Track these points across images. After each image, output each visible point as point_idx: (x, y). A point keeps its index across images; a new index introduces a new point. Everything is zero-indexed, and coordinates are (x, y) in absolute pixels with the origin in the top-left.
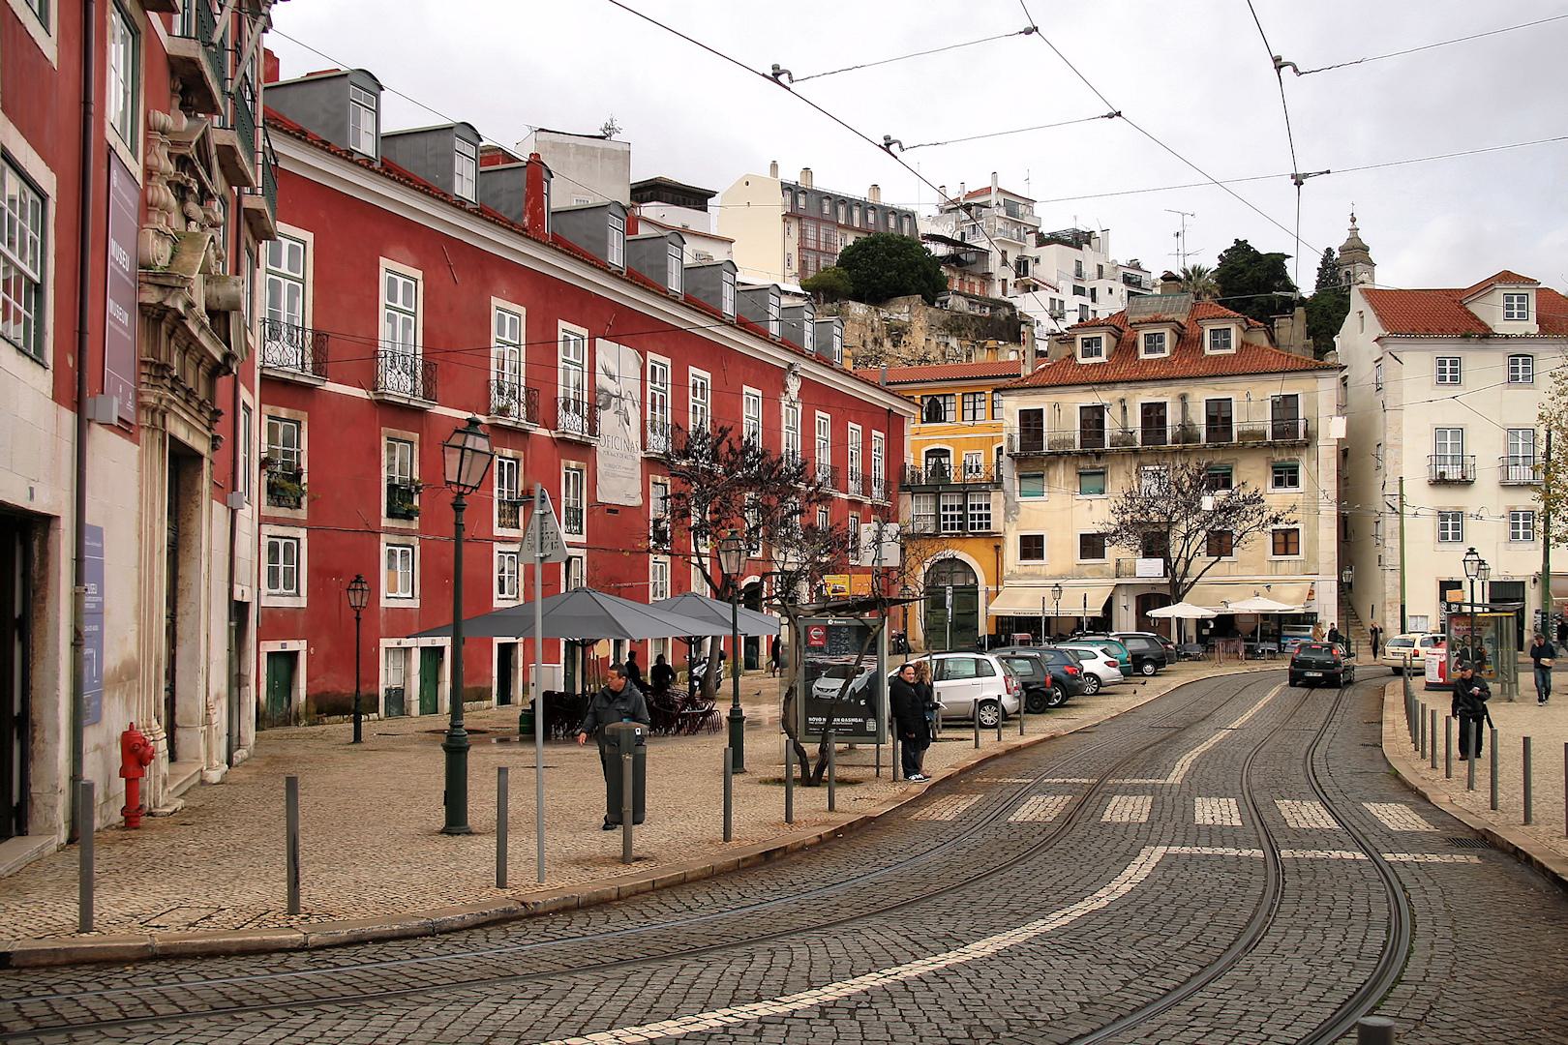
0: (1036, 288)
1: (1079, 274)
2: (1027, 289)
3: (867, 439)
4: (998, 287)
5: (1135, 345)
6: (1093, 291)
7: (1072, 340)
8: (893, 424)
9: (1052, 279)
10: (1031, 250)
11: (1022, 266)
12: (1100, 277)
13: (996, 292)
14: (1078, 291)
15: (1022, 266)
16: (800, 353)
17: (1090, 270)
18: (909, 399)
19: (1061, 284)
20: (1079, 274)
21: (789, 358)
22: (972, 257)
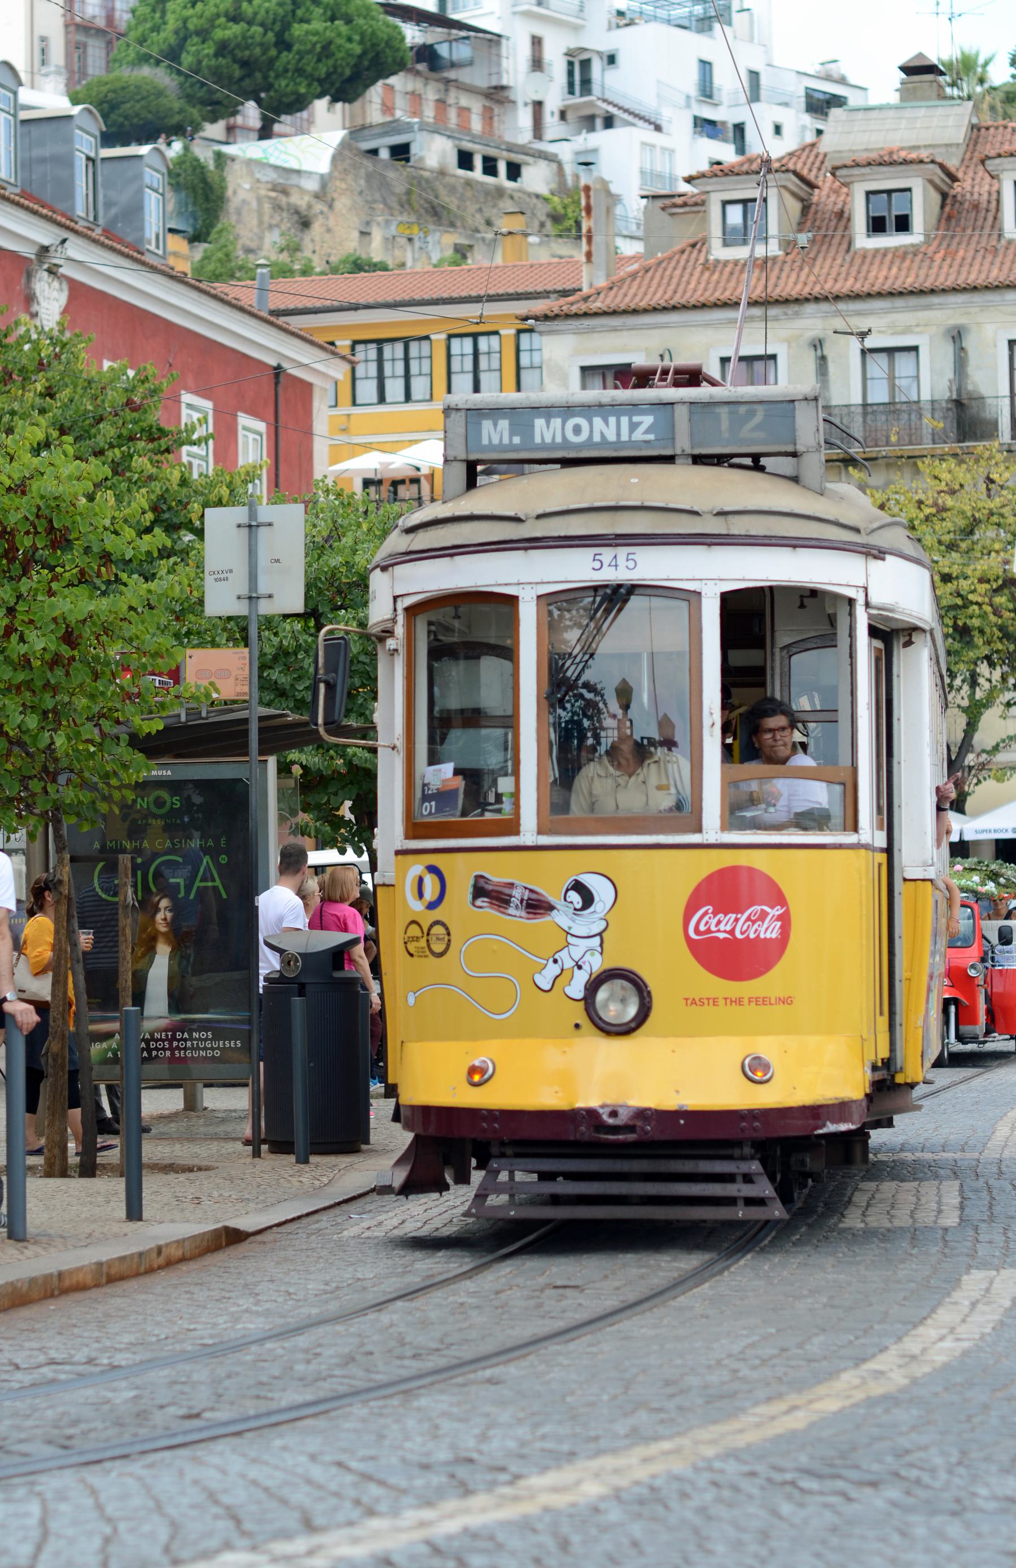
0: (609, 122)
1: (707, 91)
2: (589, 122)
3: (225, 438)
4: (524, 118)
5: (842, 217)
6: (739, 129)
7: (697, 205)
8: (282, 398)
9: (645, 100)
10: (598, 39)
11: (580, 72)
12: (754, 93)
13: (519, 126)
14: (706, 127)
15: (580, 72)
16: (67, 225)
17: (728, 81)
18: (329, 347)
19: (666, 115)
20: (707, 91)
21: (42, 234)
22: (462, 52)
